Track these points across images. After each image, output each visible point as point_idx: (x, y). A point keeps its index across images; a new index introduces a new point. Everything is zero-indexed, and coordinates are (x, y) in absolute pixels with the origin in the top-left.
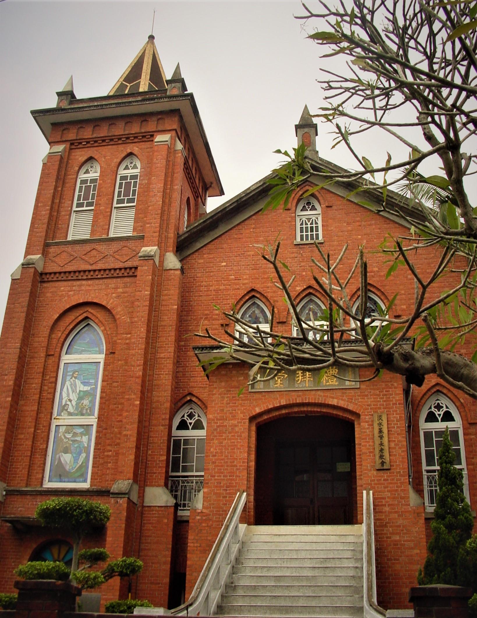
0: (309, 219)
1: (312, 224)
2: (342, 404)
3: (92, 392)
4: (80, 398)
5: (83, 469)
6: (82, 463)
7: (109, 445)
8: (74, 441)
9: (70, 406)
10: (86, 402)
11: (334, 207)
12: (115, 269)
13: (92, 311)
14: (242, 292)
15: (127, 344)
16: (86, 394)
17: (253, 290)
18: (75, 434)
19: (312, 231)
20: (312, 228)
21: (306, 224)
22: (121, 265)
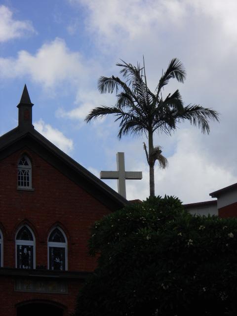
0: (23, 171)
1: (25, 174)
20: (25, 177)
21: (22, 174)
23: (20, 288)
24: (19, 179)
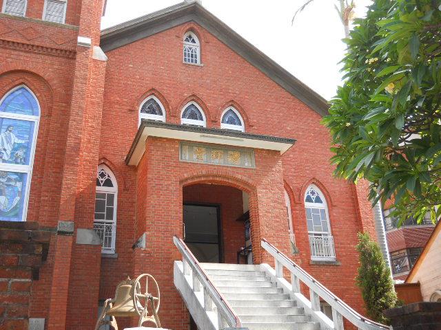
0: (190, 48)
1: (192, 52)
2: (244, 178)
3: (26, 145)
4: (15, 149)
5: (18, 210)
6: (17, 205)
7: (45, 191)
8: (7, 185)
9: (5, 154)
10: (20, 153)
11: (211, 44)
12: (52, 49)
13: (29, 79)
14: (144, 90)
15: (62, 111)
16: (20, 146)
17: (153, 89)
18: (9, 180)
19: (192, 57)
22: (57, 47)
23: (188, 156)
24: (185, 56)
